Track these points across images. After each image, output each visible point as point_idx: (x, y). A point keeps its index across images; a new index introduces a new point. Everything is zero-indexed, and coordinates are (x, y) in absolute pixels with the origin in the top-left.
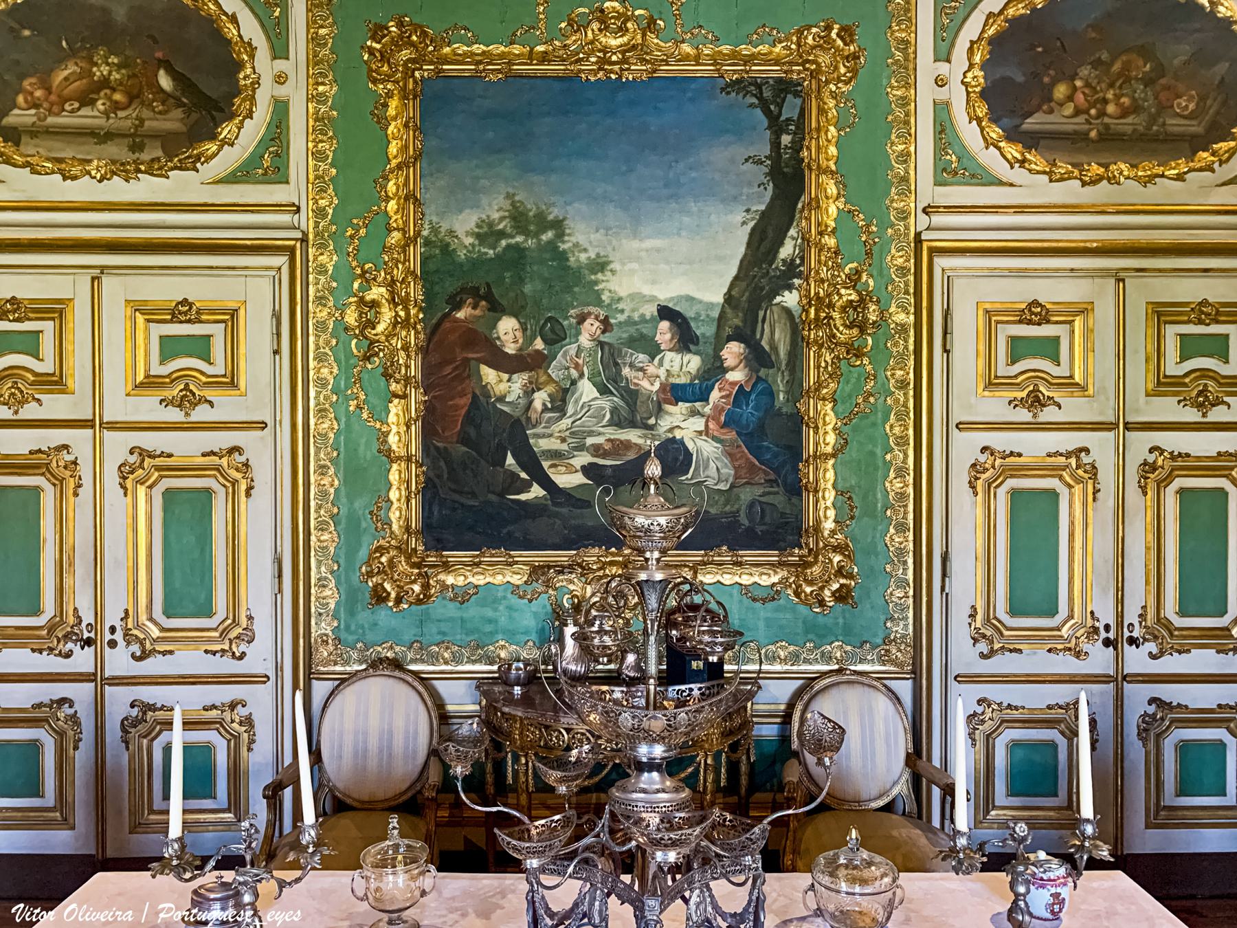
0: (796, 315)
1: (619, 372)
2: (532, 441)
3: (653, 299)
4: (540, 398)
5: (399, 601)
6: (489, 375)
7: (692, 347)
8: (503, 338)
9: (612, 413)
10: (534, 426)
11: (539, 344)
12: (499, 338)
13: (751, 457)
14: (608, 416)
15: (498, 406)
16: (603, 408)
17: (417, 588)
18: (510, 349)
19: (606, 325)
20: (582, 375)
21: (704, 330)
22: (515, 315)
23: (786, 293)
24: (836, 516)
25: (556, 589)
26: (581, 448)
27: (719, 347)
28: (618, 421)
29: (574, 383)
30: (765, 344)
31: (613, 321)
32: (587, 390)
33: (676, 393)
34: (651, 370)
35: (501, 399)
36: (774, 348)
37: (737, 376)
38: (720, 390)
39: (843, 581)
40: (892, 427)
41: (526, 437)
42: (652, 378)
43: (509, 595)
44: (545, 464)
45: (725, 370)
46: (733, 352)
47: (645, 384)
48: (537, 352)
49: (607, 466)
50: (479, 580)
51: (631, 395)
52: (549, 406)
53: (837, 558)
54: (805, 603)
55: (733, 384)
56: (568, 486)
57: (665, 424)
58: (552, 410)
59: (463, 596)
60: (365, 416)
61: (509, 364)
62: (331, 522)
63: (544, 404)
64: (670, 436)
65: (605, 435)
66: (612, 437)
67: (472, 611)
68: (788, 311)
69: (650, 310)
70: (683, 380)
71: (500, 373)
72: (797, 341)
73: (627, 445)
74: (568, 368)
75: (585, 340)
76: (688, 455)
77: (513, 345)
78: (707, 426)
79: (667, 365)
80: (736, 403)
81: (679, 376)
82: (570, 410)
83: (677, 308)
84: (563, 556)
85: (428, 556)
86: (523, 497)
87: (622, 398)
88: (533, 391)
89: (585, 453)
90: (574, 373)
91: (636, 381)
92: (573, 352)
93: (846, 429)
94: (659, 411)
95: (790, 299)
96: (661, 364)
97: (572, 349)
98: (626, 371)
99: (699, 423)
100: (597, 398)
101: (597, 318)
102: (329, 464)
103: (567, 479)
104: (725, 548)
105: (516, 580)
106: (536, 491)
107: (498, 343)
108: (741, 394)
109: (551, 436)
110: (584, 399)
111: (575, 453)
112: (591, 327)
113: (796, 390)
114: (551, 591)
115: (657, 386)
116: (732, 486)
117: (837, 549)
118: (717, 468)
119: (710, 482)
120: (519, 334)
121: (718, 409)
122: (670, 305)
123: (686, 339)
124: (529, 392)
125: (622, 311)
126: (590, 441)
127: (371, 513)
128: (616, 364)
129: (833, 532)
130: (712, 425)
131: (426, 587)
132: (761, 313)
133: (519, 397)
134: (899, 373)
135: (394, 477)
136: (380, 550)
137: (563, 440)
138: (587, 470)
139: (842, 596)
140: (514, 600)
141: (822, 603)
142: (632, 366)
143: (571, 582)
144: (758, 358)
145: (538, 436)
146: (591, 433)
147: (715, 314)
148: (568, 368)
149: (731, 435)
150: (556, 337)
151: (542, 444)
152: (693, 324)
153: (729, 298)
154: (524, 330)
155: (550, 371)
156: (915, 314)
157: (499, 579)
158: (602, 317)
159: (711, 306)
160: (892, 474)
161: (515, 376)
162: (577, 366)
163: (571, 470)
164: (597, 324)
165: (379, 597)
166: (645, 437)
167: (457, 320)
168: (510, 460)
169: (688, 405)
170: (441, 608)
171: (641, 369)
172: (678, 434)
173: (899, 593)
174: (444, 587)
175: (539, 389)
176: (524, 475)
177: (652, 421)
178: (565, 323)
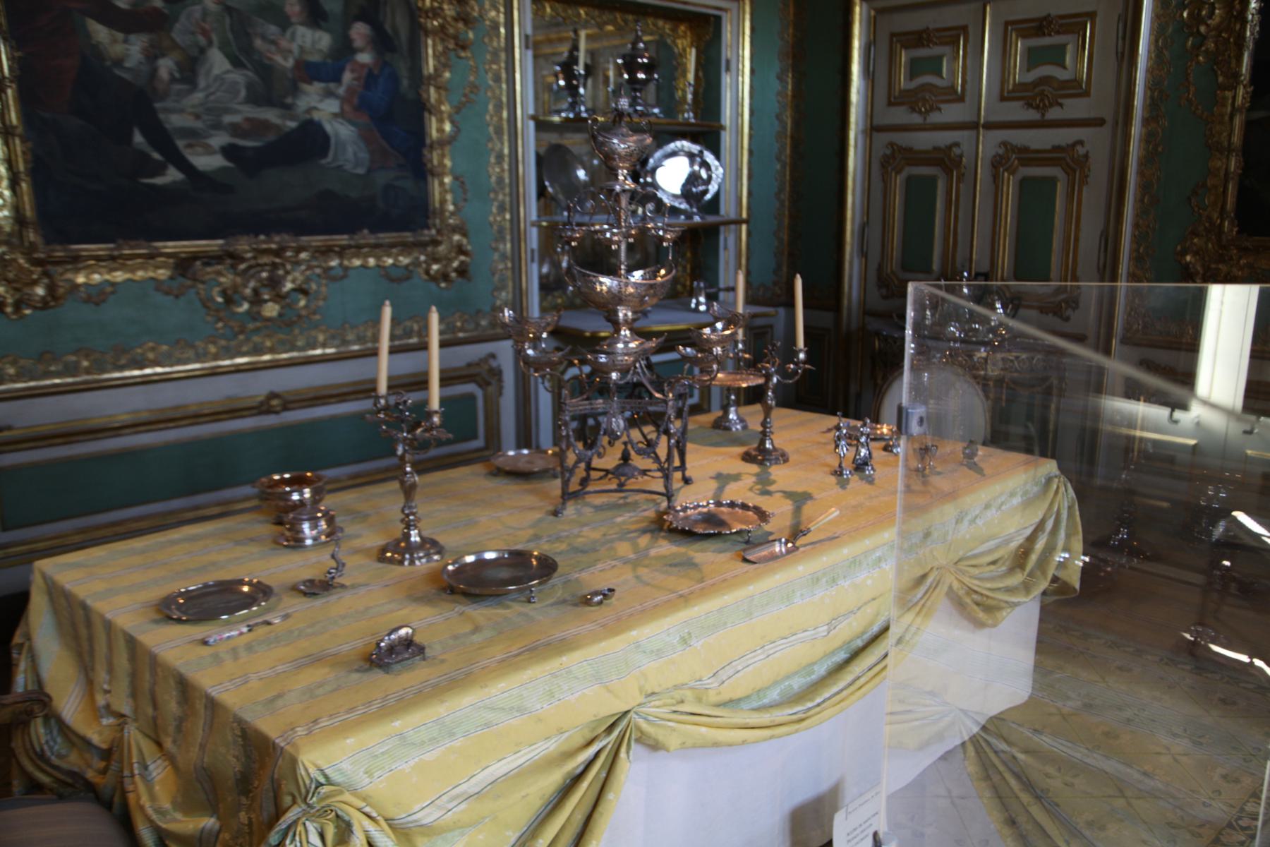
2: (162, 116)
4: (166, 66)
5: (18, 306)
6: (100, 33)
14: (243, 93)
15: (117, 72)
17: (40, 291)
20: (210, 43)
25: (203, 282)
26: (217, 126)
27: (347, 26)
28: (255, 98)
29: (202, 51)
30: (388, 27)
32: (218, 62)
33: (309, 71)
34: (284, 43)
35: (119, 63)
37: (365, 58)
38: (353, 71)
39: (462, 258)
40: (492, 117)
42: (286, 53)
44: (180, 144)
45: (354, 51)
46: (360, 31)
47: (278, 59)
49: (244, 148)
50: (119, 276)
51: (265, 71)
52: (177, 75)
53: (456, 237)
54: (434, 279)
55: (363, 66)
56: (208, 168)
57: (302, 103)
58: (182, 80)
59: (97, 296)
63: (171, 74)
64: (308, 117)
65: (242, 113)
70: (315, 58)
71: (114, 32)
72: (417, 32)
73: (264, 126)
74: (193, 33)
76: (326, 137)
78: (342, 108)
79: (299, 41)
82: (202, 83)
84: (212, 245)
85: (53, 251)
86: (158, 181)
88: (156, 57)
90: (202, 40)
91: (269, 55)
92: (198, 15)
93: (457, 118)
94: (295, 91)
96: (293, 38)
98: (258, 43)
99: (332, 106)
100: (228, 72)
103: (208, 162)
105: (163, 274)
108: (369, 78)
109: (182, 111)
110: (216, 71)
111: (213, 132)
113: (418, 79)
114: (201, 286)
115: (290, 63)
116: (369, 171)
117: (455, 229)
119: (348, 167)
121: (350, 90)
124: (152, 55)
126: (228, 119)
129: (453, 214)
130: (347, 108)
131: (51, 289)
134: (494, 67)
137: (197, 117)
138: (228, 151)
139: (462, 272)
142: (264, 38)
143: (219, 273)
144: (383, 42)
145: (168, 111)
146: (228, 111)
151: (175, 121)
155: (174, 35)
156: (505, 14)
157: (140, 274)
161: (133, 37)
162: (205, 33)
163: (209, 151)
168: (138, 138)
169: (322, 85)
171: (274, 42)
172: (316, 116)
173: (501, 266)
174: (76, 287)
175: (163, 55)
176: (156, 156)
177: (289, 100)
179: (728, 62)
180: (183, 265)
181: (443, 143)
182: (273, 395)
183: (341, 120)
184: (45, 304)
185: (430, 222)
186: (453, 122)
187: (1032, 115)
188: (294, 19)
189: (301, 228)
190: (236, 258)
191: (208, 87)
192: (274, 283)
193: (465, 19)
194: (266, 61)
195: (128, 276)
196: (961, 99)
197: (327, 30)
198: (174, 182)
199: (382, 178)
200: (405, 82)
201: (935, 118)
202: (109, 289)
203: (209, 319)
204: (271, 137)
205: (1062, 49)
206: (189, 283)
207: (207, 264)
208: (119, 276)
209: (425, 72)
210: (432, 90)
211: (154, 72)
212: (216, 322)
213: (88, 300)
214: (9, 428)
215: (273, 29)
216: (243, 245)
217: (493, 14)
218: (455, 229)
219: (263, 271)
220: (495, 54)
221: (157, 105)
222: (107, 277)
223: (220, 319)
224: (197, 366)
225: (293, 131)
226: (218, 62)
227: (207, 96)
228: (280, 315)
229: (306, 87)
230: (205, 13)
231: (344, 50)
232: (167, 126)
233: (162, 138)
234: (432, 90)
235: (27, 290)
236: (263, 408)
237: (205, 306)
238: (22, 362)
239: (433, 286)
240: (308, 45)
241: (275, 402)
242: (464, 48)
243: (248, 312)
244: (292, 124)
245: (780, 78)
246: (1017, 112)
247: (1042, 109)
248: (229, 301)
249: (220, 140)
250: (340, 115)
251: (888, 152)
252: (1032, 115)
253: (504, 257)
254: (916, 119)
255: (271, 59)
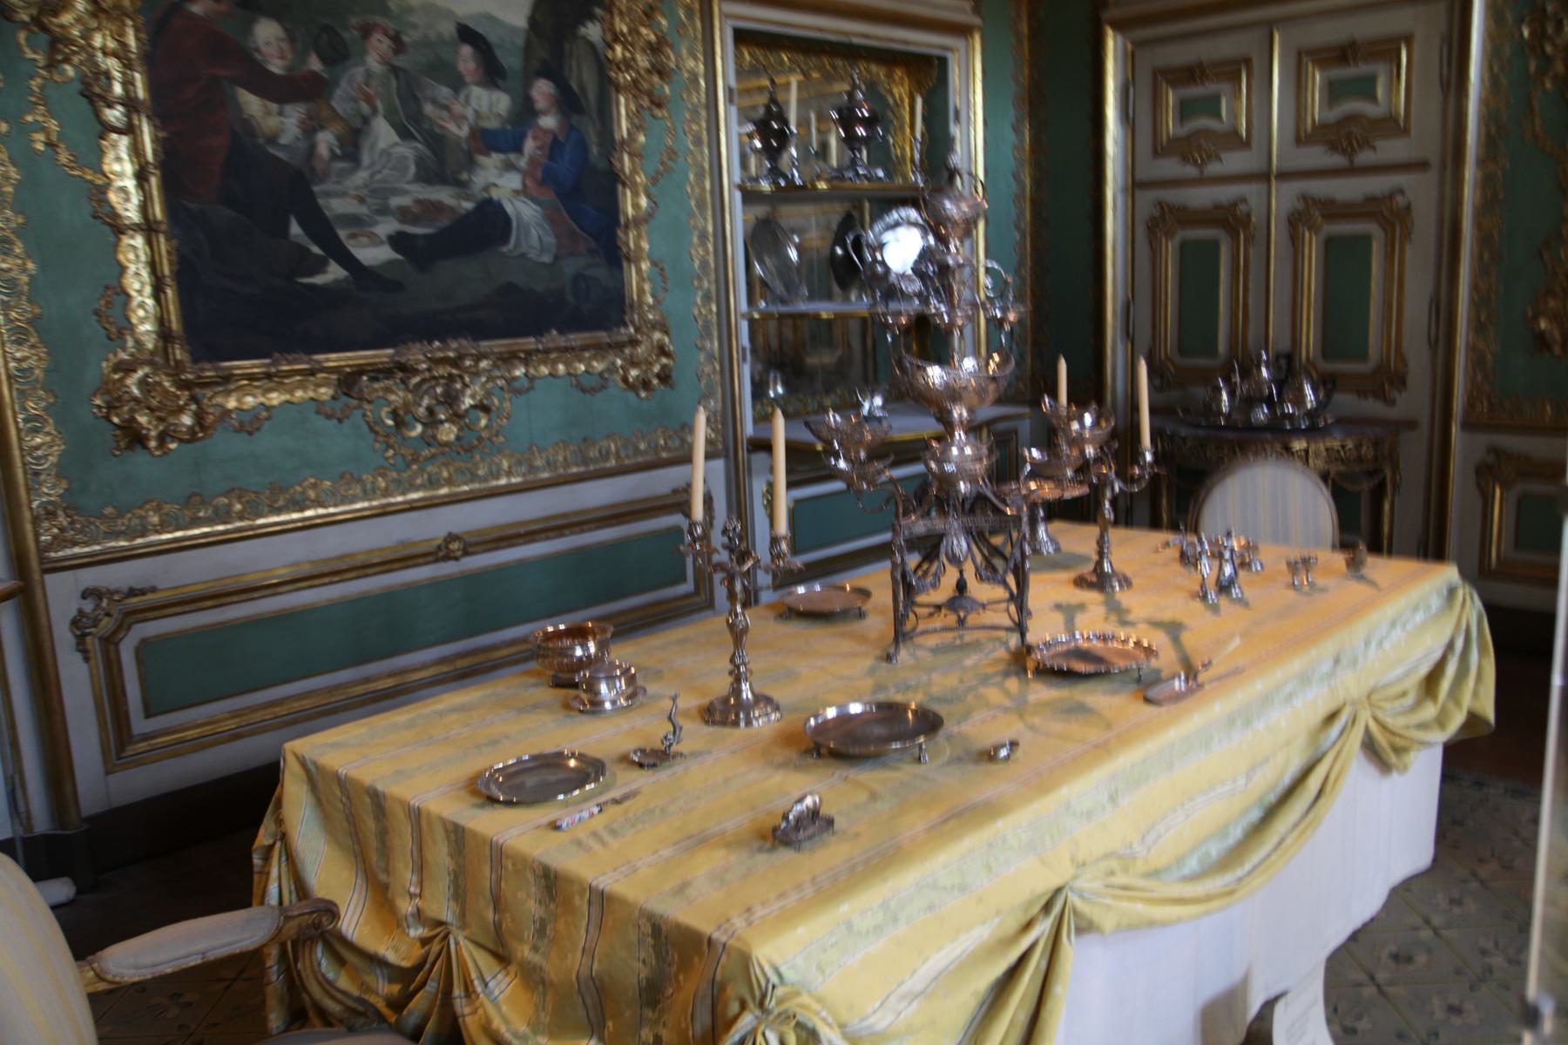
0: (600, 50)
1: (420, 110)
2: (321, 202)
3: (449, 14)
4: (325, 141)
5: (162, 438)
6: (252, 103)
7: (500, 82)
8: (264, 49)
9: (417, 164)
10: (322, 181)
11: (315, 64)
12: (258, 50)
13: (570, 222)
14: (412, 169)
15: (272, 150)
16: (405, 158)
17: (187, 420)
18: (276, 67)
19: (398, 45)
21: (511, 60)
22: (276, 16)
23: (590, 25)
24: (652, 289)
25: (369, 402)
26: (384, 211)
27: (527, 86)
29: (366, 121)
30: (574, 85)
31: (405, 39)
32: (383, 133)
33: (487, 140)
34: (457, 108)
35: (272, 140)
36: (583, 89)
37: (548, 122)
38: (535, 138)
39: (664, 360)
41: (312, 196)
42: (459, 119)
43: (313, 416)
44: (342, 234)
46: (542, 90)
47: (452, 127)
48: (314, 75)
49: (415, 237)
51: (437, 141)
52: (338, 151)
53: (657, 335)
54: (631, 387)
55: (546, 131)
57: (479, 179)
59: (251, 424)
60: (64, 157)
61: (279, 90)
62: (31, 329)
63: (332, 151)
64: (486, 195)
65: (413, 193)
66: (421, 197)
67: (266, 441)
68: (592, 46)
69: (448, 29)
70: (493, 124)
72: (607, 87)
73: (437, 208)
75: (373, 62)
76: (507, 220)
77: (278, 62)
78: (524, 185)
79: (474, 104)
80: (551, 157)
81: (489, 119)
82: (366, 159)
83: (480, 30)
84: (384, 355)
85: (203, 370)
86: (318, 280)
87: (428, 145)
89: (391, 219)
90: (365, 108)
91: (442, 123)
93: (653, 190)
94: (471, 164)
95: (593, 31)
96: (467, 101)
97: (359, 73)
98: (429, 109)
99: (513, 181)
100: (396, 144)
101: (386, 33)
102: (12, 237)
103: (373, 254)
104: (554, 332)
106: (335, 272)
107: (258, 56)
108: (554, 146)
109: (344, 194)
110: (382, 145)
111: (379, 218)
112: (379, 44)
113: (610, 144)
114: (367, 406)
115: (464, 132)
116: (556, 258)
117: (654, 326)
118: (539, 236)
119: (532, 255)
120: (285, 46)
121: (533, 162)
122: (471, 25)
123: (492, 73)
124: (310, 129)
125: (415, 26)
126: (396, 202)
127: (97, 313)
128: (416, 99)
130: (529, 183)
131: (199, 417)
132: (567, 46)
133: (298, 139)
134: (695, 127)
135: (127, 257)
136: (127, 368)
137: (361, 200)
138: (397, 241)
139: (665, 377)
140: (321, 422)
141: (646, 384)
142: (435, 102)
143: (388, 390)
144: (568, 102)
145: (328, 194)
147: (520, 41)
148: (355, 100)
149: (549, 196)
150: (338, 55)
151: (336, 206)
152: (498, 53)
153: (533, 21)
154: (291, 38)
155: (334, 104)
158: (392, 33)
159: (513, 30)
160: (695, 240)
161: (288, 108)
162: (369, 100)
163: (375, 241)
164: (387, 41)
165: (135, 438)
166: (458, 197)
167: (193, 16)
168: (295, 229)
169: (501, 156)
170: (222, 443)
171: (446, 108)
172: (495, 194)
174: (227, 413)
175: (322, 128)
176: (316, 250)
177: (464, 176)
178: (346, 35)
179: (957, 113)
180: (347, 382)
181: (637, 222)
182: (452, 537)
183: (523, 198)
184: (192, 437)
185: (627, 319)
186: (649, 196)
187: (1337, 160)
188: (468, 79)
189: (479, 331)
190: (407, 369)
191: (373, 163)
192: (451, 399)
193: (661, 71)
194: (438, 130)
195: (287, 397)
196: (1246, 144)
197: (506, 91)
198: (336, 281)
199: (570, 267)
200: (594, 150)
201: (1214, 168)
202: (264, 414)
203: (377, 445)
204: (445, 222)
205: (1371, 80)
206: (355, 402)
207: (375, 379)
208: (275, 398)
209: (617, 137)
210: (626, 158)
211: (312, 148)
212: (387, 450)
213: (240, 429)
214: (153, 590)
215: (444, 91)
216: (416, 355)
217: (691, 63)
218: (654, 326)
219: (437, 385)
220: (695, 112)
221: (316, 189)
222: (262, 399)
223: (389, 446)
224: (366, 504)
225: (469, 214)
226: (383, 133)
227: (372, 176)
228: (458, 438)
229: (482, 159)
230: (369, 75)
231: (525, 112)
232: (327, 213)
233: (321, 229)
234: (626, 158)
235: (172, 420)
236: (441, 553)
237: (372, 429)
238: (167, 508)
239: (631, 395)
240: (484, 109)
241: (455, 546)
242: (659, 105)
243: (422, 436)
244: (468, 205)
245: (1016, 129)
246: (1317, 156)
247: (1349, 152)
248: (400, 423)
249: (386, 227)
250: (523, 192)
251: (1300, 206)
252: (1337, 160)
253: (710, 357)
254: (1190, 171)
255: (442, 127)
